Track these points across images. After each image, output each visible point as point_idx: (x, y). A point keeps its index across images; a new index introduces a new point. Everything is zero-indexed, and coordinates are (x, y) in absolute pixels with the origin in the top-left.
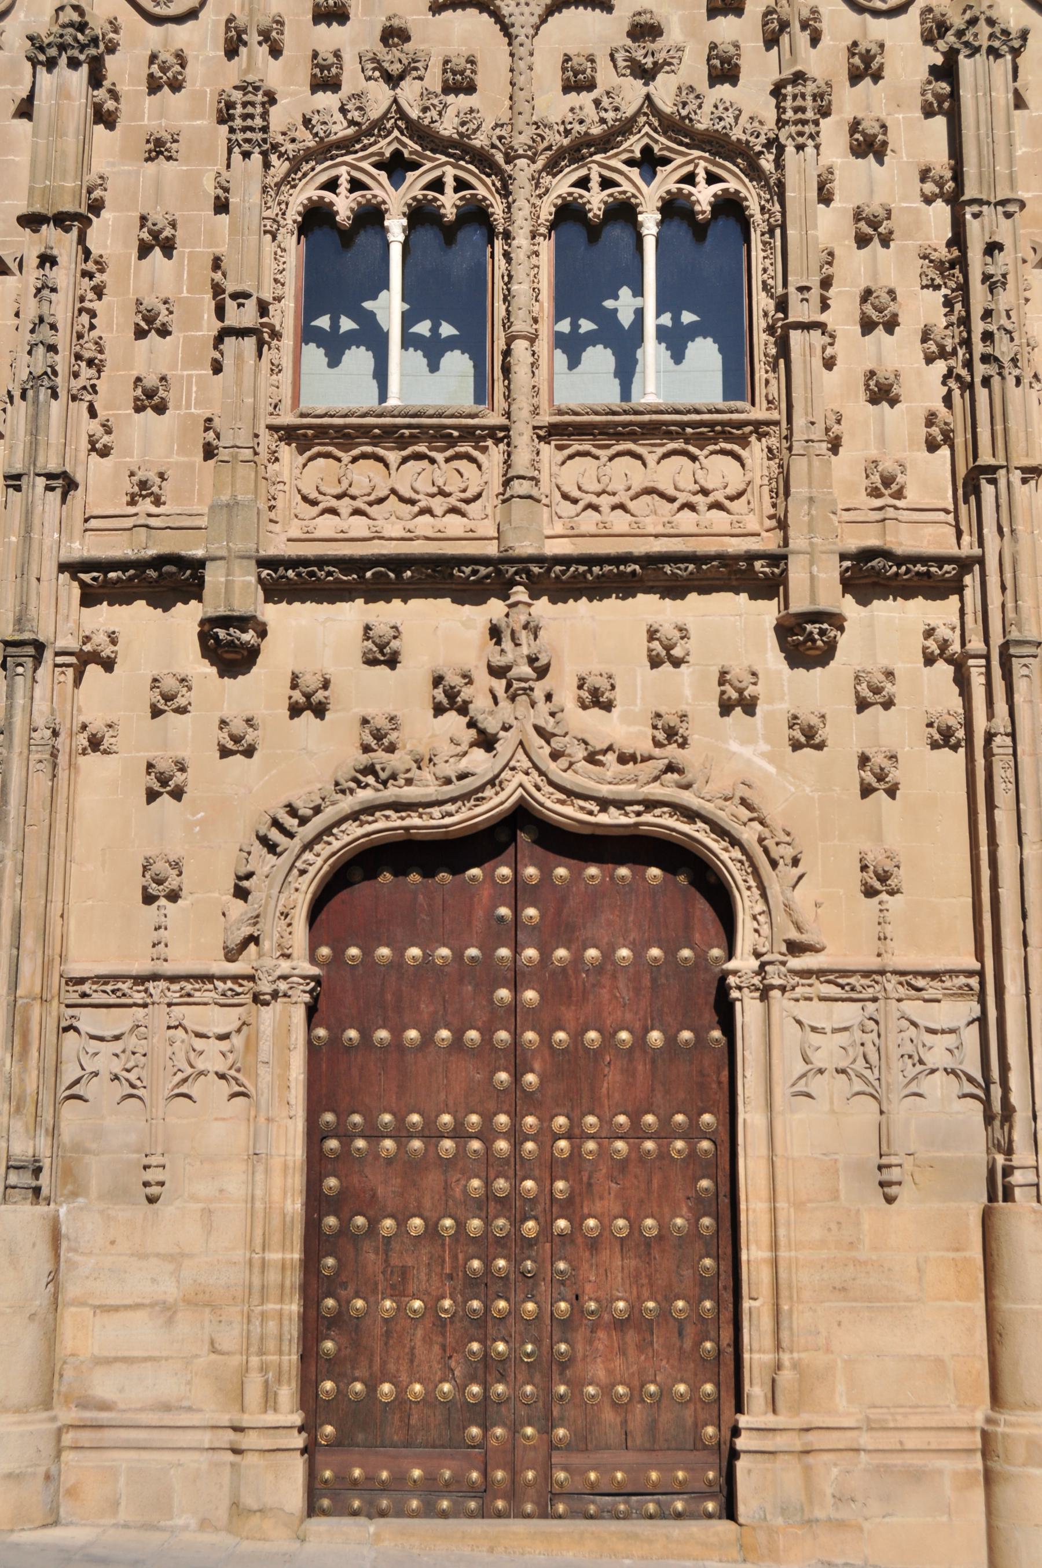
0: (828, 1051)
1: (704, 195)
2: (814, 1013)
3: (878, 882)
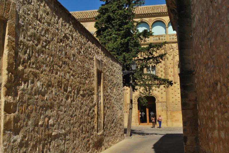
0: (160, 105)
1: (153, 65)
2: (159, 104)
3: (162, 98)
